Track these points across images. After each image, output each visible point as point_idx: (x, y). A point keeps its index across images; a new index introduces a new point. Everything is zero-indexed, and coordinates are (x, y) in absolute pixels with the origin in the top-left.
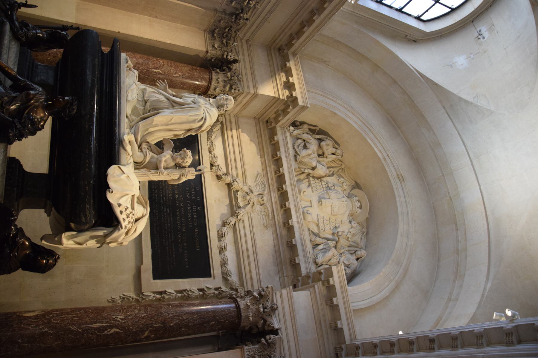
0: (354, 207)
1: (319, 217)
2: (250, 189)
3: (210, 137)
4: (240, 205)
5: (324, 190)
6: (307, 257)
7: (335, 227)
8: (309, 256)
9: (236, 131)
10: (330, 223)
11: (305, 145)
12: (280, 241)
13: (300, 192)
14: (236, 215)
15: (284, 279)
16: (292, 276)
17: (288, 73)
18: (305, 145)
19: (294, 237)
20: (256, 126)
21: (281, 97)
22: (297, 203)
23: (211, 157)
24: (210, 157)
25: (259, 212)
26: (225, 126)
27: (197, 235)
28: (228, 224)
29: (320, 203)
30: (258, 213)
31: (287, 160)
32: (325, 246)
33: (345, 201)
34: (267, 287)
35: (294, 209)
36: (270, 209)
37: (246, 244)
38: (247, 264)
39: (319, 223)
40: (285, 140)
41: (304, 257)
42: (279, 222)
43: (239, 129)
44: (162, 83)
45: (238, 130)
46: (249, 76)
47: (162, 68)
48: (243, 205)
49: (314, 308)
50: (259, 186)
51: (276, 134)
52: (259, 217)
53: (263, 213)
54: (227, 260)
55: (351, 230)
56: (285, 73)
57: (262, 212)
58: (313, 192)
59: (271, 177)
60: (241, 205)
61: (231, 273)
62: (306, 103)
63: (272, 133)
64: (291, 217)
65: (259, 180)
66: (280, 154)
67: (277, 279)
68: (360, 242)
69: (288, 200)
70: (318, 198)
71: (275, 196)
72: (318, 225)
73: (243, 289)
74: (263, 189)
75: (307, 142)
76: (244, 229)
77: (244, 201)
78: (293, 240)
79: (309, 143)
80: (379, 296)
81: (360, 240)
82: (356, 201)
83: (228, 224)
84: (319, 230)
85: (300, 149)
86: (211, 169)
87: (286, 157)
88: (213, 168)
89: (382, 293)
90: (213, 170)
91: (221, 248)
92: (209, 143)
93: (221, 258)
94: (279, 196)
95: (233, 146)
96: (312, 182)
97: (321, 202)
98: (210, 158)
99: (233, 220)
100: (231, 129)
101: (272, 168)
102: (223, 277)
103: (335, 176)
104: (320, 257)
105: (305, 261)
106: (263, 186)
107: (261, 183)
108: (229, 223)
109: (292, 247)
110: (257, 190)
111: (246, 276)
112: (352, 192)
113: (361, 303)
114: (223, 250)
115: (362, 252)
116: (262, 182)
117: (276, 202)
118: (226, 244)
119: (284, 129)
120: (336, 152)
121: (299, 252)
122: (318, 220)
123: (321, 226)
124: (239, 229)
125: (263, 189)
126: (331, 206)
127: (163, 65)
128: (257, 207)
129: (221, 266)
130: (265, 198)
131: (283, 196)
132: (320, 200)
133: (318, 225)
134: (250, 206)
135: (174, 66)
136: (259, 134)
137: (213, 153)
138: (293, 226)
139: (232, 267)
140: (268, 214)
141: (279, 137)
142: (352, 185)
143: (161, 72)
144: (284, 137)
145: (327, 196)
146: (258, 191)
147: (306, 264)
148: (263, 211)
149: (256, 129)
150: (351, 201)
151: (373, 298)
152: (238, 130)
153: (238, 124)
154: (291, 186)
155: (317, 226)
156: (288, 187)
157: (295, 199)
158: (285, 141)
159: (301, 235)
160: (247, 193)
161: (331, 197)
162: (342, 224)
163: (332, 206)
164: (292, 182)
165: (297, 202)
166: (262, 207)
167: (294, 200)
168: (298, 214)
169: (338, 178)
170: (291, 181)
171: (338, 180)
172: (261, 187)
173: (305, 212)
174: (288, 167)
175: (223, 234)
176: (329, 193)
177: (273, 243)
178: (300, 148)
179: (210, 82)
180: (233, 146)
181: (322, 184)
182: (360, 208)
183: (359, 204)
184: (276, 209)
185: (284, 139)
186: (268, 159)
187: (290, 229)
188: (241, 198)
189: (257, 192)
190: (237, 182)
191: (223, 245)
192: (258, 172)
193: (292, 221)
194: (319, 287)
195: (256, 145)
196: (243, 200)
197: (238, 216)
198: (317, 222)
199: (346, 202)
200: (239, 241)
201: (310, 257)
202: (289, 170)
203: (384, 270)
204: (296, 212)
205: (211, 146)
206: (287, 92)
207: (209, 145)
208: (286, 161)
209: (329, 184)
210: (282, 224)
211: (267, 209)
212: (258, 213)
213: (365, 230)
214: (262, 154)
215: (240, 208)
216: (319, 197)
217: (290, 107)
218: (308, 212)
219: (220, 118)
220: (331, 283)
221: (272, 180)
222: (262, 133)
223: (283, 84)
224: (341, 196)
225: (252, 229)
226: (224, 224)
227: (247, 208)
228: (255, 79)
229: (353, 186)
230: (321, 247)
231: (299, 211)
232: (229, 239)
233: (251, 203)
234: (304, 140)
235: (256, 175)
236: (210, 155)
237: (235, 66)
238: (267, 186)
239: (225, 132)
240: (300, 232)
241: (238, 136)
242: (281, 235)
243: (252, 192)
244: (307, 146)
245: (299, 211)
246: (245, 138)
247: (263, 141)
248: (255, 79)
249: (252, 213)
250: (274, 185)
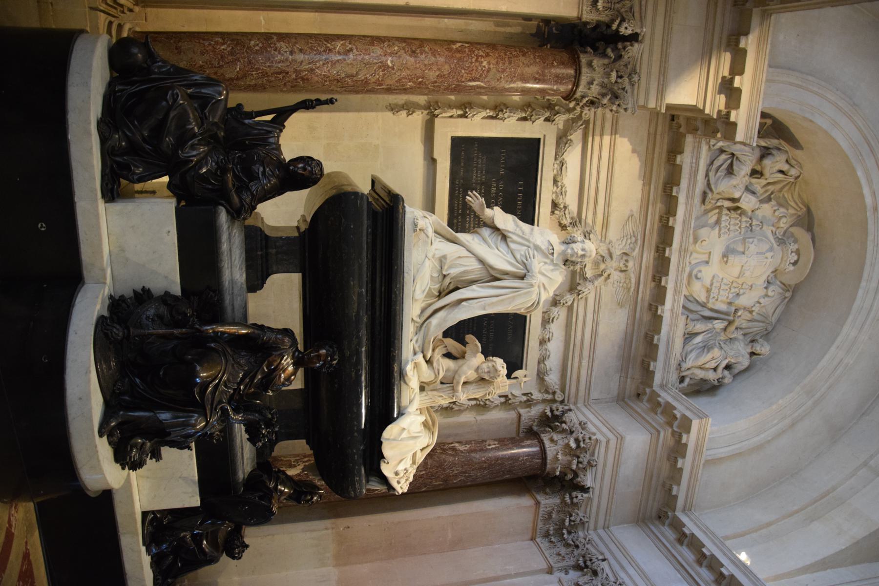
0: (783, 262)
1: (714, 281)
2: (609, 250)
3: (560, 154)
4: (587, 275)
5: (740, 233)
6: (669, 364)
7: (738, 294)
8: (673, 362)
9: (610, 137)
10: (730, 289)
11: (731, 165)
12: (636, 328)
13: (696, 240)
14: (577, 291)
15: (627, 381)
16: (640, 381)
17: (738, 68)
18: (731, 165)
19: (659, 333)
20: (650, 121)
21: (707, 111)
22: (681, 281)
23: (556, 192)
24: (553, 193)
25: (616, 283)
26: (591, 126)
27: (511, 320)
28: (562, 304)
29: (725, 259)
30: (614, 283)
31: (686, 204)
32: (706, 337)
33: (769, 257)
34: (590, 438)
35: (673, 289)
36: (633, 281)
37: (583, 332)
38: (576, 360)
39: (711, 289)
40: (696, 163)
41: (665, 364)
42: (643, 300)
43: (615, 134)
44: (476, 197)
45: (613, 137)
46: (655, 70)
47: (486, 77)
48: (592, 275)
49: (650, 457)
50: (627, 240)
51: (681, 152)
52: (614, 289)
53: (621, 285)
55: (762, 301)
56: (726, 97)
57: (620, 283)
58: (719, 237)
59: (651, 224)
60: (589, 273)
62: (751, 138)
63: (675, 150)
64: (663, 303)
65: (630, 228)
66: (678, 192)
67: (616, 378)
68: (771, 315)
69: (667, 275)
70: (723, 249)
71: (649, 257)
72: (708, 291)
74: (631, 245)
75: (737, 158)
76: (584, 310)
77: (595, 269)
78: (656, 337)
79: (739, 161)
80: (756, 439)
81: (772, 311)
82: (792, 252)
83: (562, 304)
84: (708, 297)
85: (719, 177)
86: (553, 212)
87: (687, 197)
88: (556, 212)
89: (762, 436)
90: (554, 216)
91: (543, 339)
92: (556, 166)
93: (541, 354)
94: (655, 259)
95: (599, 167)
96: (724, 218)
97: (728, 259)
98: (554, 195)
99: (569, 298)
100: (602, 135)
101: (658, 208)
102: (538, 374)
103: (773, 203)
104: (689, 360)
105: (664, 368)
106: (633, 239)
107: (632, 234)
108: (564, 304)
109: (651, 348)
110: (621, 247)
111: (572, 376)
112: (792, 229)
113: (722, 450)
114: (545, 342)
115: (763, 349)
116: (633, 232)
117: (647, 267)
118: (552, 333)
119: (699, 142)
120: (789, 170)
121: (659, 353)
122: (712, 284)
123: (714, 291)
124: (577, 310)
125: (631, 245)
126: (742, 266)
127: (489, 70)
128: (616, 276)
129: (539, 363)
130: (631, 264)
131: (665, 235)
132: (725, 256)
133: (708, 291)
134: (603, 278)
135: (508, 70)
136: (652, 137)
137: (559, 184)
138: (662, 317)
139: (553, 363)
140: (629, 287)
141: (685, 160)
142: (799, 213)
143: (482, 84)
144: (695, 158)
145: (740, 248)
146: (623, 249)
147: (664, 373)
148: (623, 281)
149: (649, 127)
150: (783, 251)
151: (744, 443)
152: (613, 137)
153: (616, 124)
154: (680, 251)
155: (707, 291)
156: (678, 222)
157: (680, 273)
158: (694, 165)
159: (671, 330)
160: (603, 257)
161: (746, 253)
162: (750, 289)
163: (744, 268)
164: (684, 244)
165: (681, 279)
166: (622, 275)
167: (677, 276)
168: (676, 297)
169: (776, 208)
170: (682, 242)
171: (775, 211)
172: (629, 241)
173: (694, 272)
174: (685, 216)
175: (551, 319)
176: (747, 244)
177: (625, 329)
178: (719, 174)
179: (576, 84)
180: (599, 167)
181: (740, 221)
182: (795, 263)
183: (796, 258)
184: (645, 278)
185: (694, 161)
186: (656, 188)
187: (657, 319)
188: (590, 265)
189: (621, 250)
190: (590, 239)
191: (547, 337)
192: (631, 211)
193: (663, 310)
194: (666, 435)
195: (640, 160)
196: (593, 267)
197: (579, 294)
198: (709, 287)
199: (771, 260)
200: (573, 328)
201: (672, 365)
202: (684, 221)
203: (781, 402)
204: (674, 295)
205: (560, 172)
206: (721, 101)
207: (555, 171)
208: (684, 205)
209: (754, 220)
210: (646, 304)
211: (630, 279)
212: (614, 283)
213: (788, 294)
214: (647, 177)
215: (585, 279)
216: (727, 247)
217: (719, 135)
218: (699, 275)
219: (586, 114)
220: (684, 441)
221: (652, 232)
222: (658, 137)
223: (720, 80)
224: (766, 247)
225: (596, 312)
226: (555, 303)
227: (596, 283)
228: (664, 75)
229: (800, 216)
230: (698, 339)
231: (679, 293)
232: (557, 329)
233: (606, 275)
234: (733, 155)
235: (627, 218)
236: (555, 188)
237: (634, 50)
238: (639, 242)
239: (590, 139)
240: (671, 326)
241: (612, 147)
242: (641, 320)
243: (611, 257)
244: (733, 171)
245: (679, 293)
246: (624, 145)
247: (655, 156)
248: (664, 78)
249: (603, 287)
250: (653, 239)
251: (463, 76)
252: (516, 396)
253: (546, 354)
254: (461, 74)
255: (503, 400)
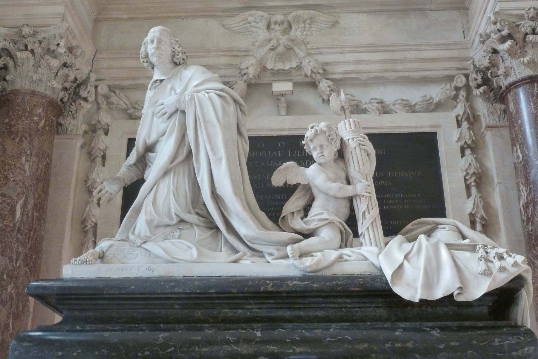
54: (403, 100)
61: (425, 96)
73: (458, 77)
93: (402, 110)
118: (372, 99)
191: (376, 105)
251: (6, 226)
252: (460, 134)
253: (399, 104)
254: (4, 227)
255: (468, 152)
